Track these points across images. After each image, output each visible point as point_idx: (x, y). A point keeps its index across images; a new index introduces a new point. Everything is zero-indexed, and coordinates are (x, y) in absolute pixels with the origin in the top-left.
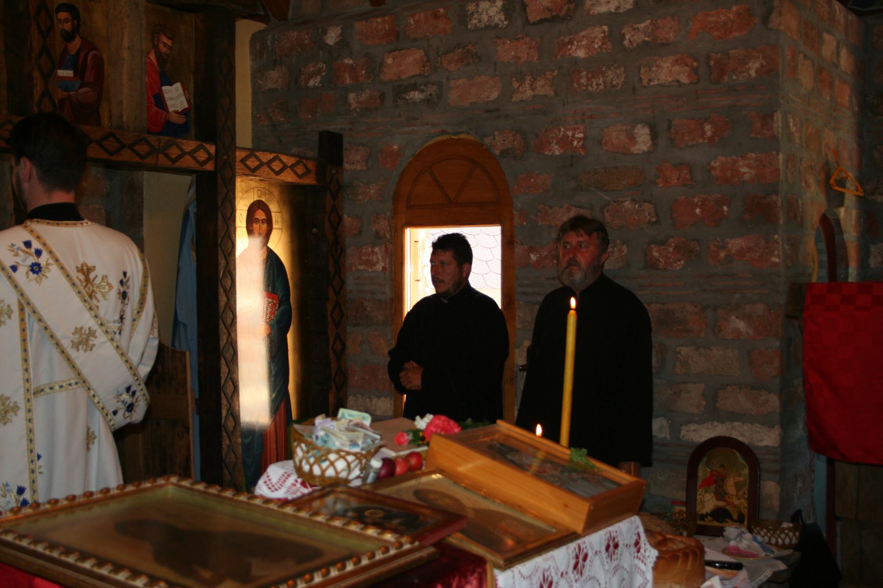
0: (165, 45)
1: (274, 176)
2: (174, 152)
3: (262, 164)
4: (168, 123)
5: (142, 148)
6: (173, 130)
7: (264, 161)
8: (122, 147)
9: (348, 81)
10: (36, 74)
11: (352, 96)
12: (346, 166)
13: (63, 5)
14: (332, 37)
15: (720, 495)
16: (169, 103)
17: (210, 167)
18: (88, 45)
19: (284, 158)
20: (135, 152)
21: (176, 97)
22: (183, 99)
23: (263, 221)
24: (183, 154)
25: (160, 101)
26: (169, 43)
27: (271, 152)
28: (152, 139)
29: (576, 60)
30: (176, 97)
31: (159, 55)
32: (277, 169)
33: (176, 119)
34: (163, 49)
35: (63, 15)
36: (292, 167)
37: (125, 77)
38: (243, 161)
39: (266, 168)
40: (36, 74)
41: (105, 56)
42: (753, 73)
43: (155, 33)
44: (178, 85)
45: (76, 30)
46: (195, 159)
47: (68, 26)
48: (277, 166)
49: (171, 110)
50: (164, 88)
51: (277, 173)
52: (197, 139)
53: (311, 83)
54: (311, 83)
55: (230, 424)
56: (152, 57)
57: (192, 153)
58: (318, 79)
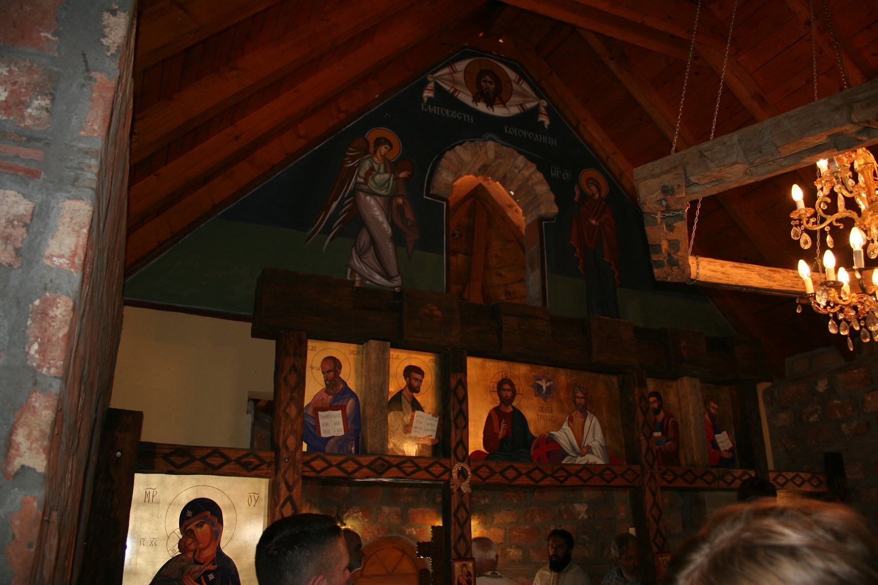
0: (714, 408)
1: (797, 488)
2: (729, 478)
3: (787, 481)
5: (709, 478)
6: (723, 462)
7: (789, 478)
9: (839, 416)
10: (642, 438)
11: (844, 426)
12: (848, 476)
13: (652, 393)
14: (822, 386)
16: (720, 445)
18: (669, 415)
19: (803, 475)
20: (705, 481)
21: (724, 441)
22: (729, 441)
25: (714, 444)
26: (716, 406)
27: (793, 472)
28: (714, 471)
30: (724, 441)
31: (710, 415)
32: (799, 483)
33: (727, 455)
34: (713, 411)
35: (652, 399)
36: (809, 480)
37: (693, 433)
38: (774, 479)
40: (642, 438)
41: (679, 420)
43: (706, 402)
44: (725, 433)
45: (660, 407)
47: (655, 405)
48: (798, 481)
49: (722, 449)
50: (716, 436)
51: (799, 486)
52: (741, 468)
53: (812, 419)
54: (812, 419)
56: (707, 417)
58: (816, 416)
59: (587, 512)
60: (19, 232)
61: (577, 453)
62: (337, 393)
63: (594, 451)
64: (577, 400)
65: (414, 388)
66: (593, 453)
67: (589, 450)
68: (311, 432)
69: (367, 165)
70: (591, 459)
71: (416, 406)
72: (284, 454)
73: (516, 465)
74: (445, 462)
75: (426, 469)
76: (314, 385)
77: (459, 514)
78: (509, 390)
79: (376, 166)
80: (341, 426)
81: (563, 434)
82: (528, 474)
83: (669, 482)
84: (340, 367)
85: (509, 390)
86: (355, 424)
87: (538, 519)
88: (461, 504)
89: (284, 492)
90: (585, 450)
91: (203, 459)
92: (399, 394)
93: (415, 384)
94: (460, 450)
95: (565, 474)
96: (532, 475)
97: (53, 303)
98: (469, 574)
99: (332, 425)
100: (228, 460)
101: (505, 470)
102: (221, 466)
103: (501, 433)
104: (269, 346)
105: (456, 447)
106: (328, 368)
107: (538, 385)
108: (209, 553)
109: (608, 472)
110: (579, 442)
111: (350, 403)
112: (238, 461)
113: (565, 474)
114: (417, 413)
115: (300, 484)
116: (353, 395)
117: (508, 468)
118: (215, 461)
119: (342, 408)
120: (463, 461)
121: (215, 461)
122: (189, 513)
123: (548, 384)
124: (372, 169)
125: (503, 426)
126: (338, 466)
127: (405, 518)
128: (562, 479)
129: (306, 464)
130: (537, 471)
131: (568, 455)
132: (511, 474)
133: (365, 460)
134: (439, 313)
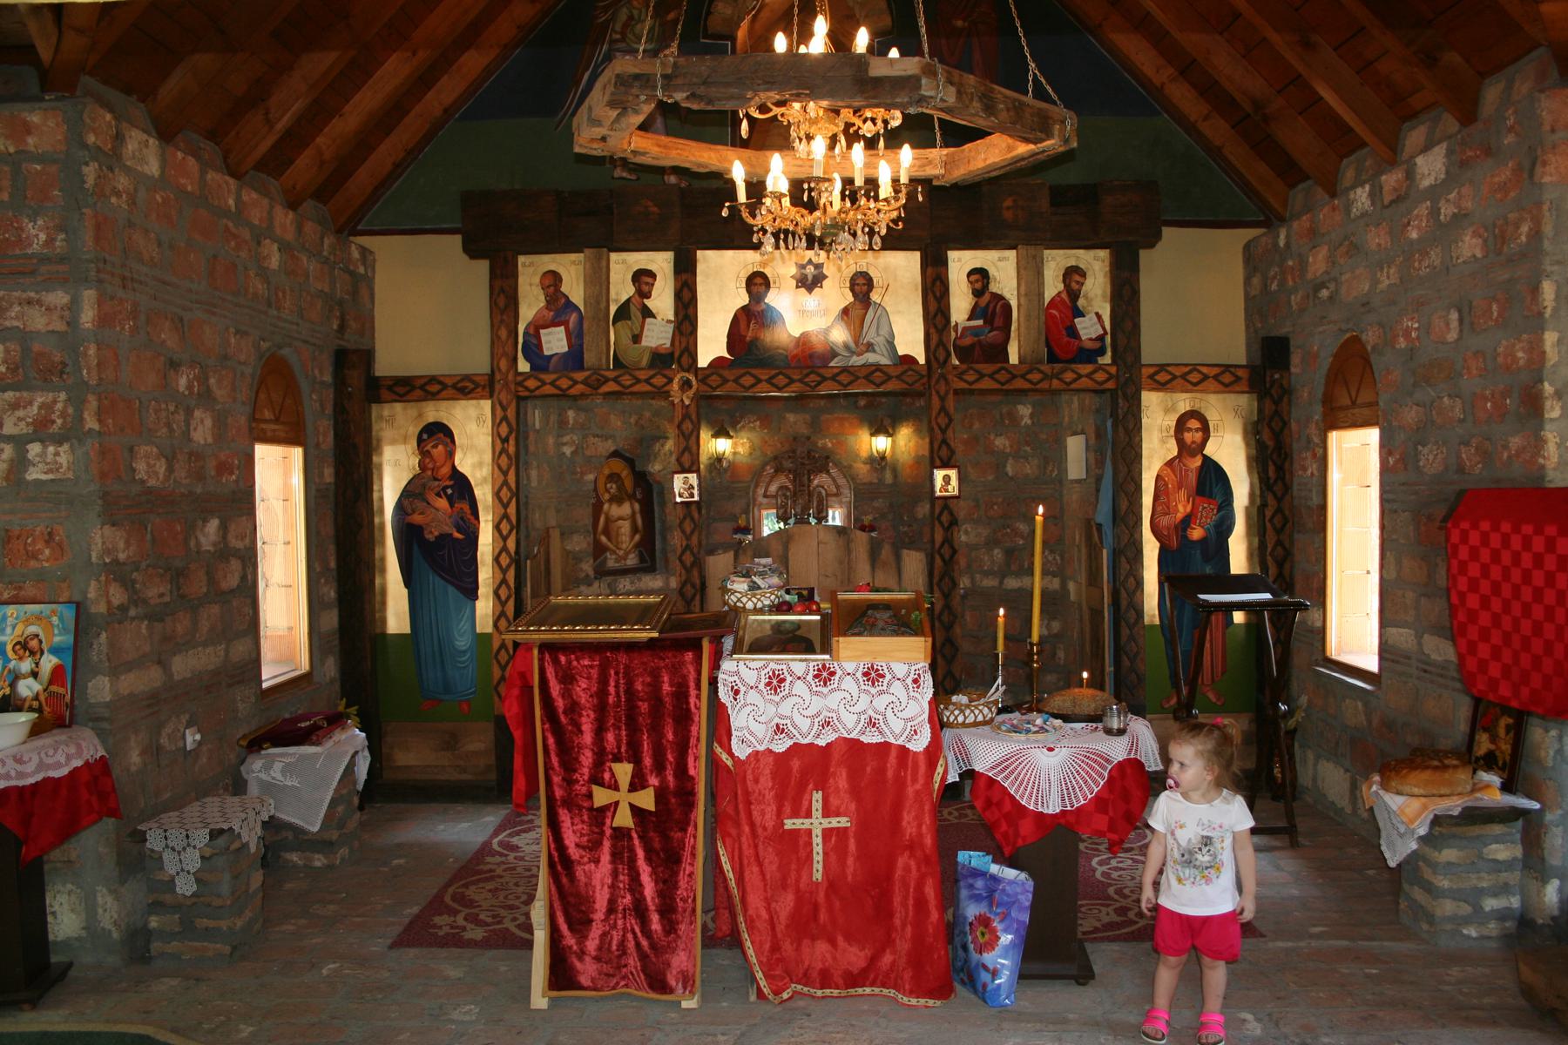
2: (1069, 376)
4: (1082, 350)
5: (1035, 377)
8: (1014, 377)
15: (1494, 739)
16: (1081, 333)
17: (1110, 385)
23: (1197, 430)
24: (1080, 376)
29: (1412, 242)
33: (1089, 345)
38: (1151, 377)
39: (1179, 380)
42: (1523, 238)
46: (1061, 380)
47: (978, 286)
55: (1132, 615)
57: (1089, 376)
59: (1032, 416)
60: (67, 313)
62: (558, 307)
65: (643, 292)
67: (870, 347)
68: (533, 350)
69: (623, 15)
70: (871, 358)
71: (647, 313)
72: (498, 377)
73: (754, 371)
74: (668, 372)
75: (647, 381)
76: (531, 305)
77: (684, 427)
79: (635, 12)
80: (565, 342)
83: (971, 384)
84: (561, 280)
86: (575, 338)
87: (977, 425)
88: (686, 416)
89: (499, 413)
91: (422, 388)
92: (629, 300)
93: (645, 288)
94: (685, 360)
97: (87, 348)
98: (692, 487)
99: (555, 342)
100: (444, 386)
102: (439, 392)
104: (483, 266)
105: (681, 356)
106: (547, 283)
108: (445, 470)
111: (573, 318)
112: (454, 386)
114: (649, 320)
115: (514, 404)
116: (576, 308)
118: (435, 388)
119: (565, 324)
120: (688, 371)
121: (435, 388)
122: (425, 436)
124: (631, 18)
126: (553, 384)
127: (816, 426)
129: (520, 384)
133: (579, 376)
134: (656, 209)
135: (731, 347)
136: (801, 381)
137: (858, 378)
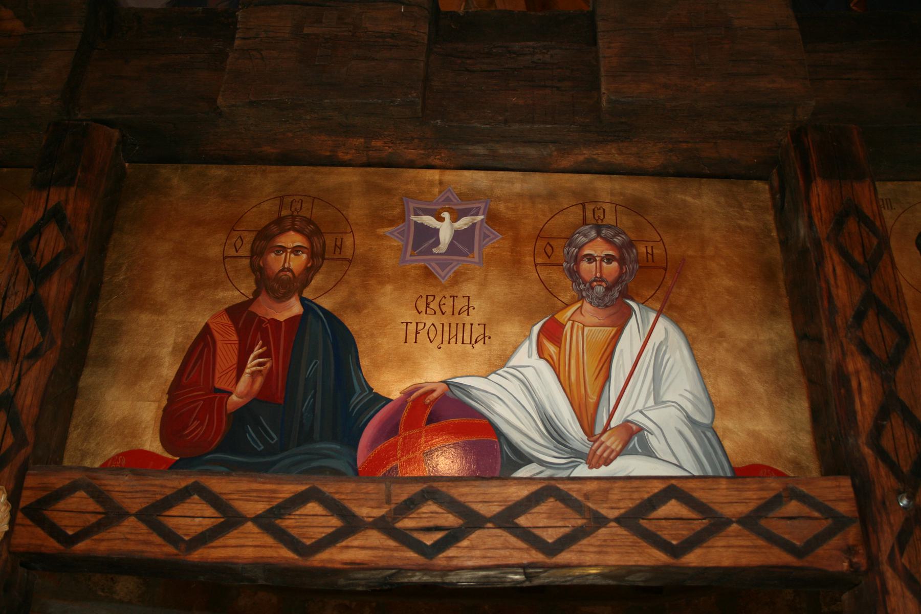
40: (856, 364)
61: (577, 454)
63: (654, 442)
64: (585, 265)
66: (648, 452)
67: (633, 437)
73: (219, 485)
78: (296, 250)
81: (514, 387)
82: (267, 522)
85: (296, 250)
90: (612, 442)
95: (450, 520)
96: (288, 523)
101: (168, 502)
103: (242, 390)
107: (421, 227)
109: (673, 508)
110: (586, 416)
113: (450, 520)
117: (182, 495)
123: (463, 223)
125: (252, 364)
128: (428, 540)
130: (313, 508)
131: (525, 459)
132: (193, 517)
135: (171, 425)
136: (384, 525)
137: (600, 521)
